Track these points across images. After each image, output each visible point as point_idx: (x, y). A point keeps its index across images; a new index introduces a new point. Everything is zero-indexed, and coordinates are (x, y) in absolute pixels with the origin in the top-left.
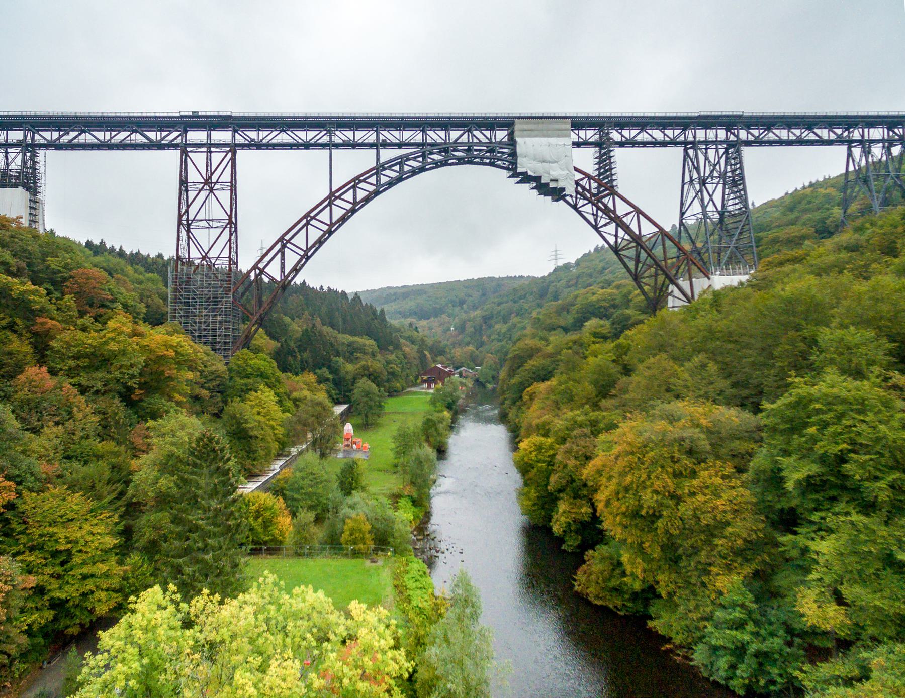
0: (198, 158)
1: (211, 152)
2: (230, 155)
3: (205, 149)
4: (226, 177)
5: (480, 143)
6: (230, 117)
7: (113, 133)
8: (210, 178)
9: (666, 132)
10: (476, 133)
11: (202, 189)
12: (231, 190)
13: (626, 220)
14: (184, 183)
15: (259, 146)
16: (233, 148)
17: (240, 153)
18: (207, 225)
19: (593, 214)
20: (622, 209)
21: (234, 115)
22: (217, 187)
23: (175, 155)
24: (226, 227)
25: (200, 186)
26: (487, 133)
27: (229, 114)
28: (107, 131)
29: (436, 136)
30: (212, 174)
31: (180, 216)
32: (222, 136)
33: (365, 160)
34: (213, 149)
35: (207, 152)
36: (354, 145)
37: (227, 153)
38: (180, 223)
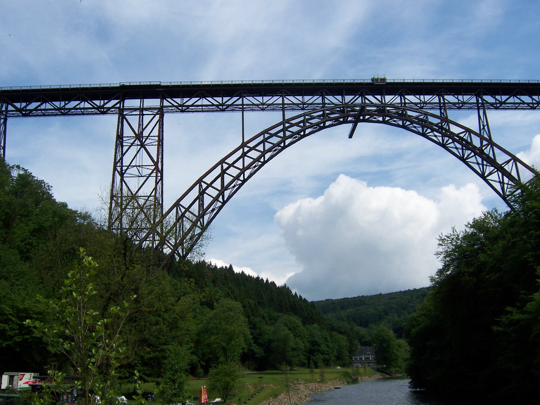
0: (134, 120)
1: (143, 115)
2: (158, 117)
3: (138, 113)
4: (156, 132)
5: (372, 104)
6: (159, 86)
7: (106, 101)
8: (142, 133)
9: (533, 97)
10: (370, 97)
11: (132, 144)
12: (159, 145)
13: (507, 168)
14: (120, 137)
15: (183, 109)
16: (161, 111)
17: (167, 117)
18: (137, 174)
19: (478, 164)
20: (501, 158)
21: (162, 84)
22: (148, 141)
23: (114, 119)
24: (150, 175)
25: (132, 141)
26: (379, 97)
27: (158, 83)
28: (62, 101)
29: (333, 100)
30: (143, 130)
31: (115, 164)
32: (155, 103)
33: (276, 117)
34: (145, 112)
35: (140, 115)
36: (263, 108)
37: (155, 115)
38: (115, 169)
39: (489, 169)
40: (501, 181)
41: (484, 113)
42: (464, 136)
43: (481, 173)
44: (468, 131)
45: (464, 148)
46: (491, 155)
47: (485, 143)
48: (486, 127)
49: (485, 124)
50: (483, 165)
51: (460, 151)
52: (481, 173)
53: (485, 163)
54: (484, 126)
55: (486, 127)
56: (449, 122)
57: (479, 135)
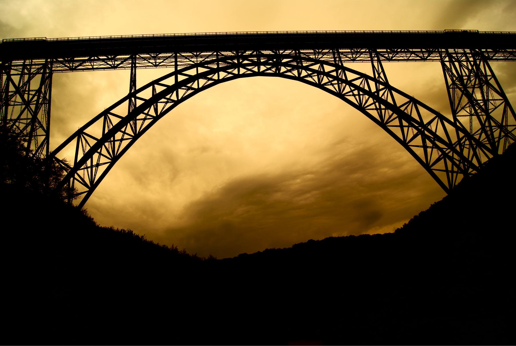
39: (411, 132)
40: (378, 107)
41: (379, 61)
42: (360, 85)
43: (357, 104)
44: (365, 77)
45: (361, 93)
46: (390, 100)
47: (381, 87)
48: (382, 75)
49: (380, 70)
50: (380, 109)
51: (357, 97)
52: (357, 104)
53: (383, 107)
54: (379, 74)
55: (382, 75)
56: (345, 69)
57: (373, 79)
